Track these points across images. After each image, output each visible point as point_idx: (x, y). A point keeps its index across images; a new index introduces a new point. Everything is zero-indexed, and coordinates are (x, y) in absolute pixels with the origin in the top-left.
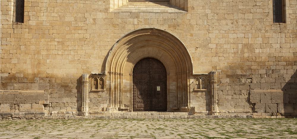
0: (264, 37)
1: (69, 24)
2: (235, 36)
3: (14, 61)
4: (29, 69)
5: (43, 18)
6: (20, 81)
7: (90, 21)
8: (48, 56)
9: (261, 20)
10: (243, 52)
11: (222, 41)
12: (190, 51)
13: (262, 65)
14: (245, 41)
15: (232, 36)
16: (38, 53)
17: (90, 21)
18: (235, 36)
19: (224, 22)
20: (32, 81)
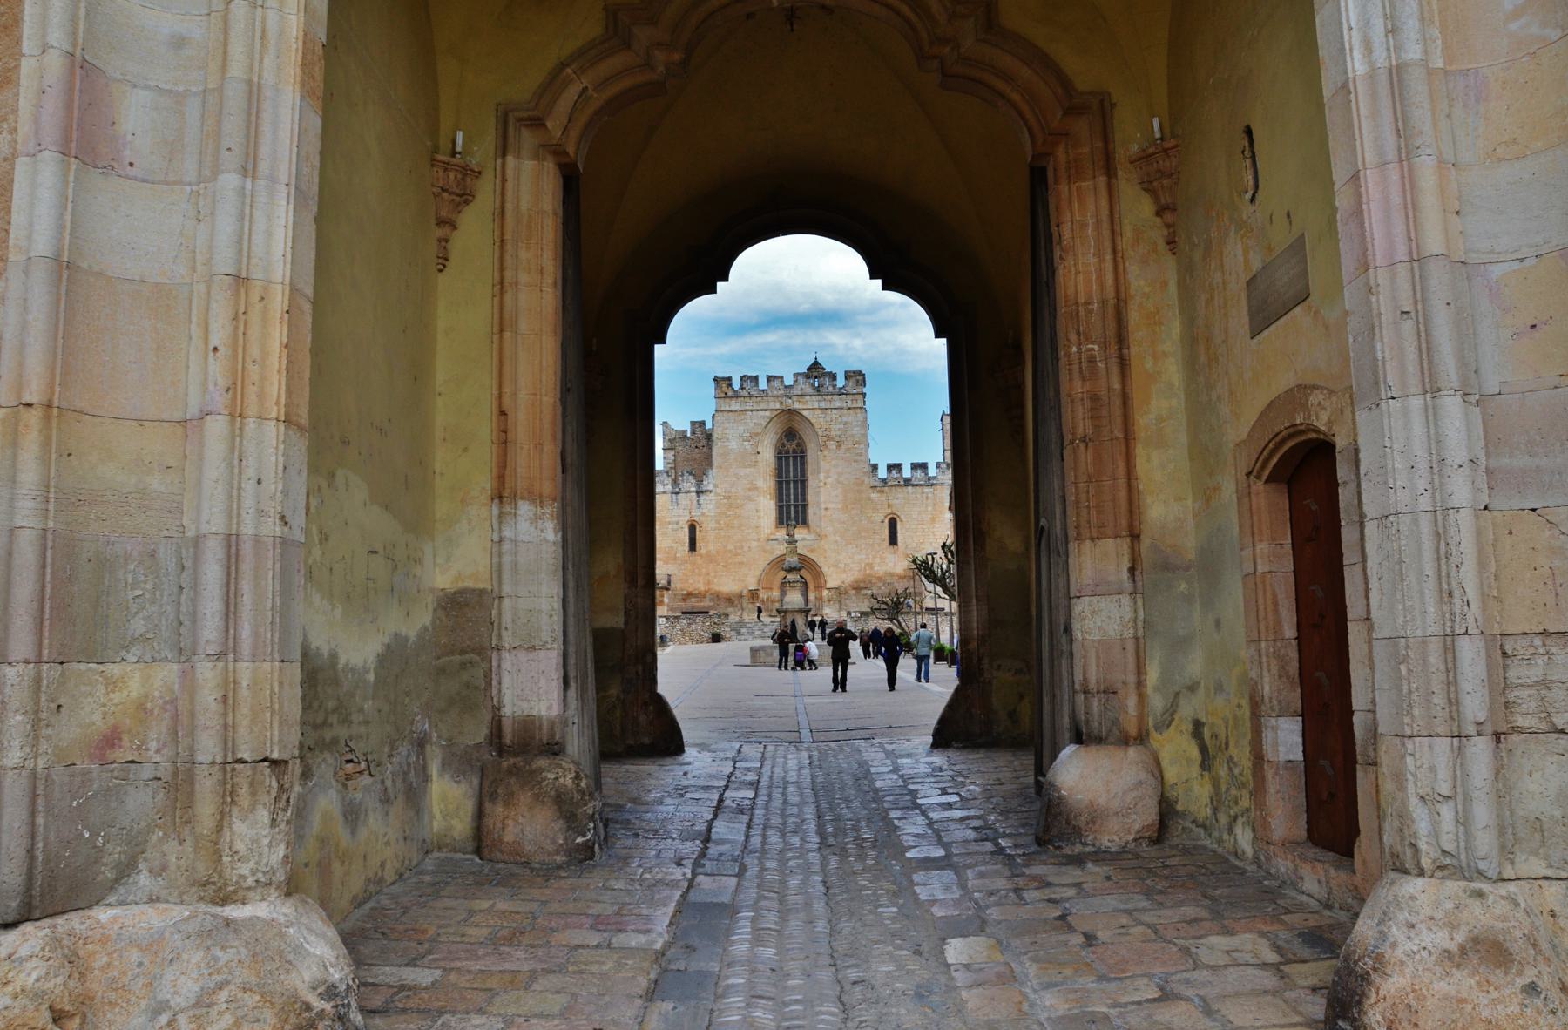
0: (881, 557)
1: (730, 551)
2: (860, 557)
3: (691, 581)
4: (701, 587)
5: (711, 547)
6: (695, 596)
7: (746, 549)
8: (715, 577)
9: (879, 545)
10: (865, 570)
11: (849, 561)
12: (825, 569)
13: (880, 579)
14: (867, 561)
15: (857, 557)
16: (708, 574)
17: (746, 549)
18: (860, 557)
19: (850, 546)
20: (704, 597)
